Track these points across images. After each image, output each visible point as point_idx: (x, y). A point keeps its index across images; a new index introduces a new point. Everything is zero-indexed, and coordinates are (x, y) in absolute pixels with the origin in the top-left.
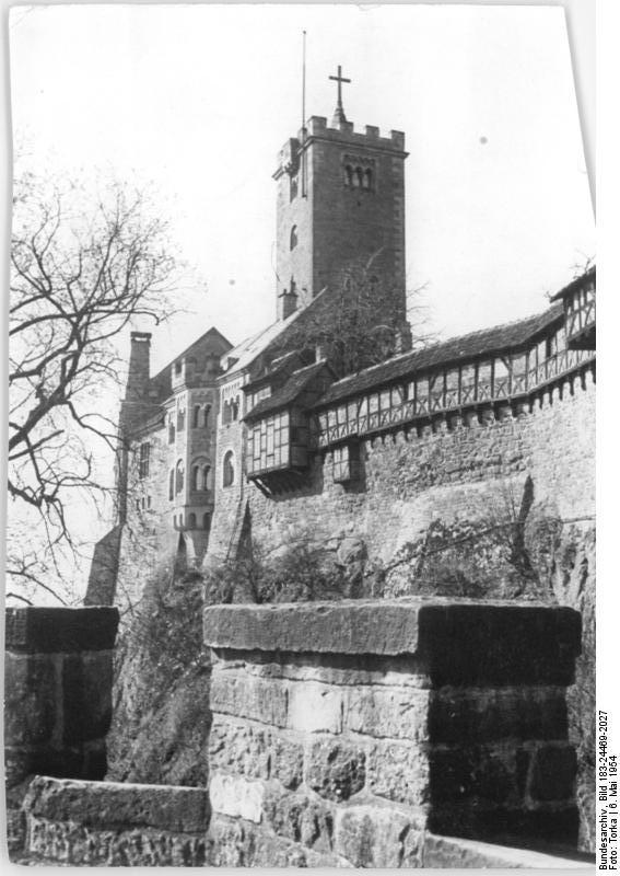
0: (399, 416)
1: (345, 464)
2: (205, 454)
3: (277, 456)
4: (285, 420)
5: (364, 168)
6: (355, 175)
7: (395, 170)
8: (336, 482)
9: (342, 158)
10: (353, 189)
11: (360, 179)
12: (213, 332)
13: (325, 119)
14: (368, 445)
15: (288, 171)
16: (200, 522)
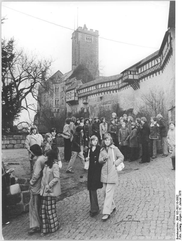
0: (95, 92)
1: (85, 100)
2: (57, 97)
3: (72, 98)
4: (74, 92)
5: (90, 38)
6: (88, 39)
7: (96, 39)
8: (84, 103)
9: (85, 36)
10: (88, 42)
11: (89, 40)
12: (59, 71)
13: (82, 27)
14: (89, 97)
15: (74, 38)
16: (57, 111)
